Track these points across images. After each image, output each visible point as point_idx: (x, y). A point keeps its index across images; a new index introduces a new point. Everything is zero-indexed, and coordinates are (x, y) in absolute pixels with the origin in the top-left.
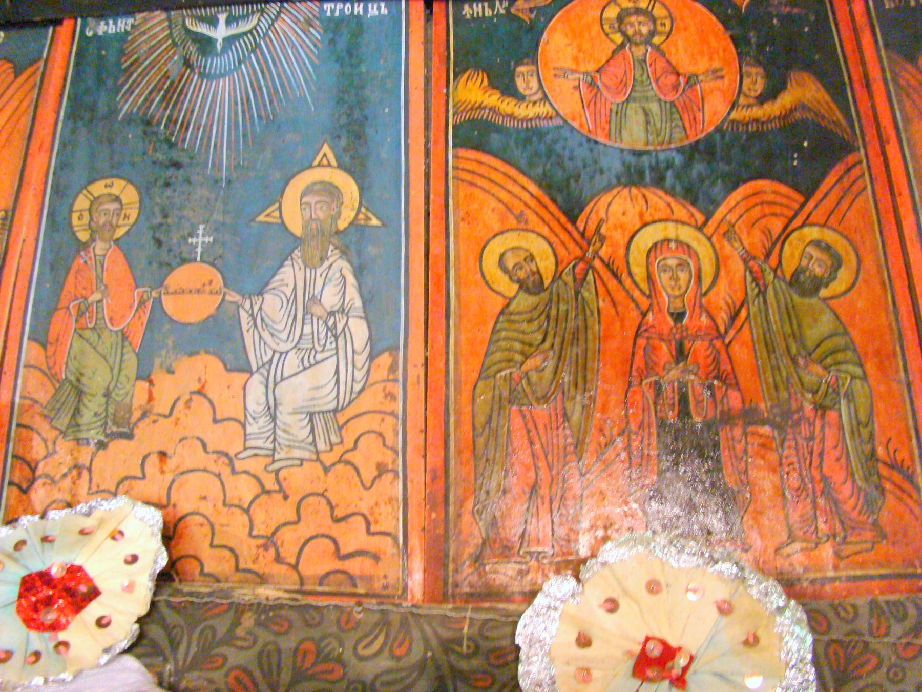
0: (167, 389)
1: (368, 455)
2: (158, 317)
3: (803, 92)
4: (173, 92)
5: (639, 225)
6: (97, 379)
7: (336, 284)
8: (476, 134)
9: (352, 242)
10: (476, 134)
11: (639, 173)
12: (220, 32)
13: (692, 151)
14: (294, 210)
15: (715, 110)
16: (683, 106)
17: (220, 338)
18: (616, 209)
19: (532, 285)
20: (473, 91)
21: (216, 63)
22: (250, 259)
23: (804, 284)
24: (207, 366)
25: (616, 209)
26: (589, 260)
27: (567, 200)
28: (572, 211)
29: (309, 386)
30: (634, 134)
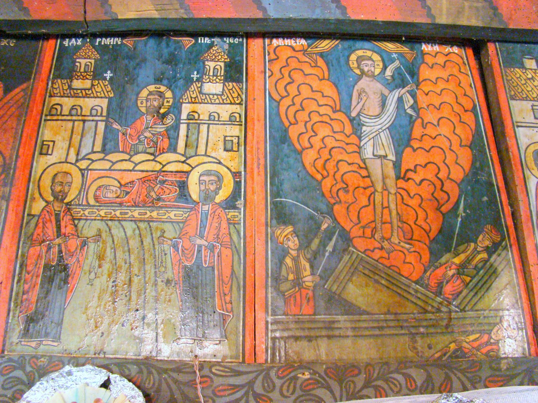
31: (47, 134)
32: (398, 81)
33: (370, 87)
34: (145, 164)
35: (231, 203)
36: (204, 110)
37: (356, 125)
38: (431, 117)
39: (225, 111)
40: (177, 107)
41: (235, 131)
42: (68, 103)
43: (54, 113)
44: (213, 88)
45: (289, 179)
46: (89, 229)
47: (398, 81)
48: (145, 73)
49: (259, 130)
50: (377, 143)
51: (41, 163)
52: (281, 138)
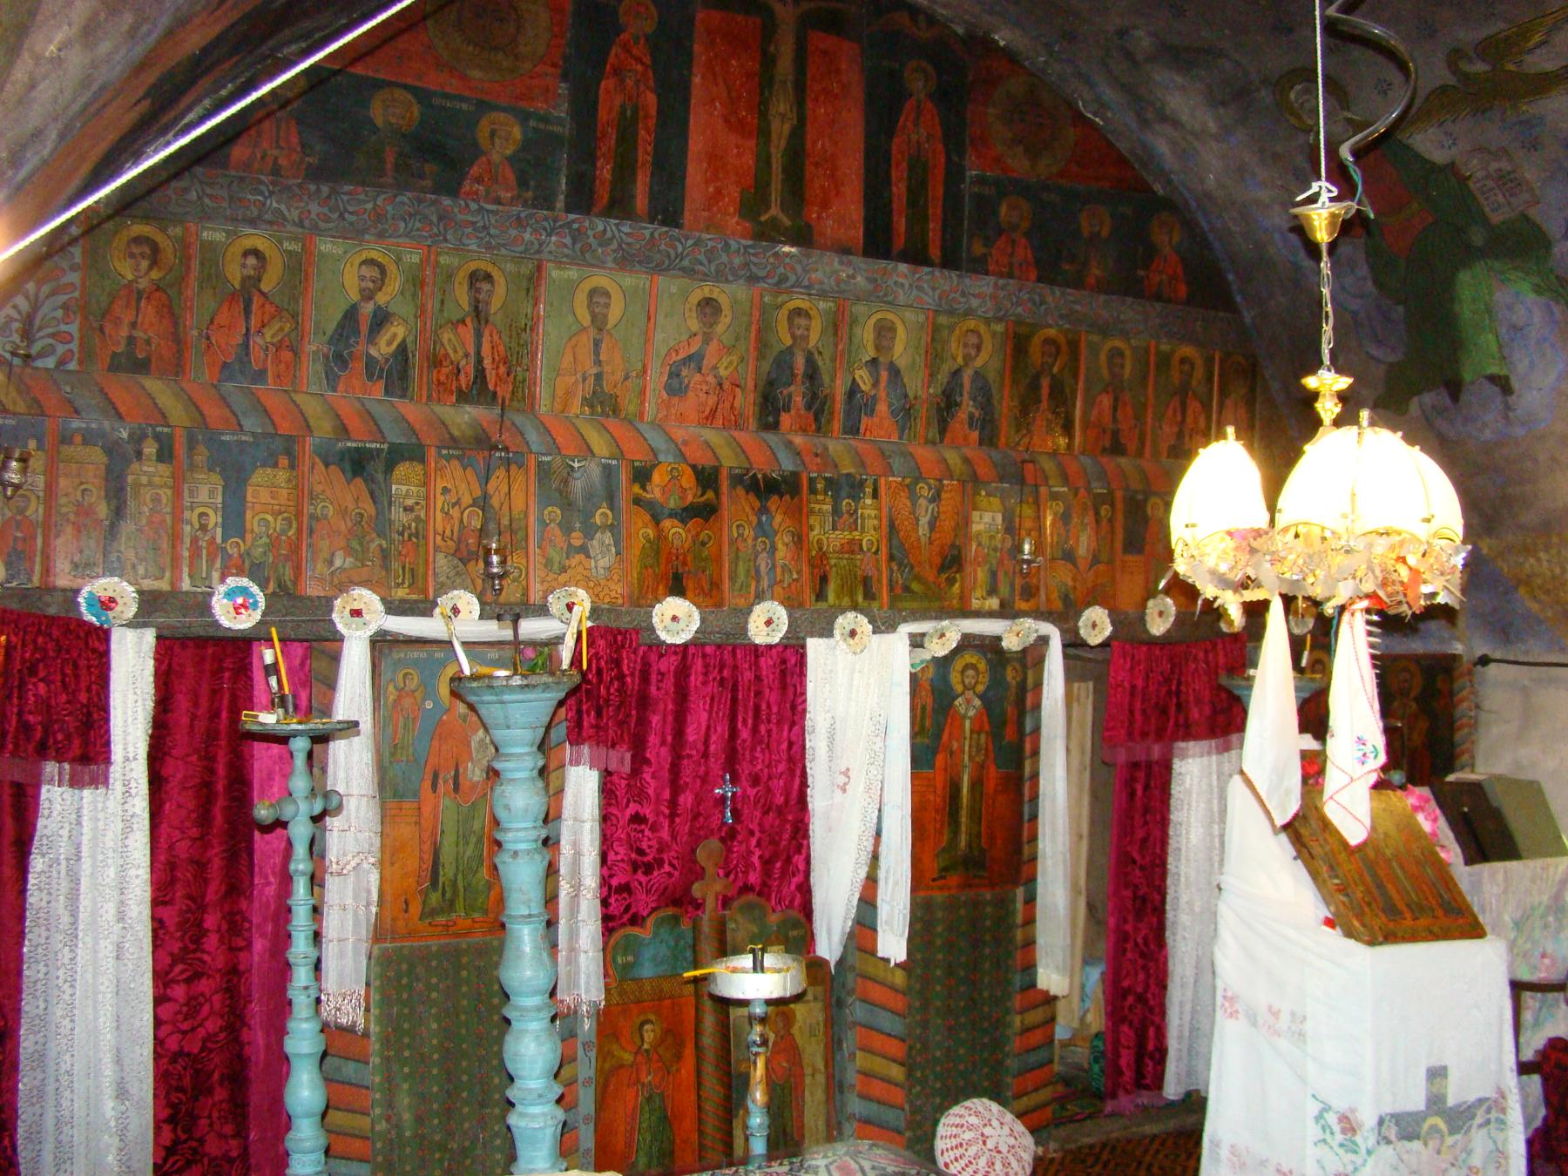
0: (574, 562)
1: (616, 577)
2: (570, 545)
3: (710, 495)
4: (566, 482)
5: (675, 530)
6: (557, 559)
7: (608, 538)
8: (637, 501)
9: (612, 528)
10: (637, 501)
11: (672, 515)
12: (576, 465)
13: (684, 509)
14: (598, 519)
15: (690, 498)
16: (683, 498)
17: (584, 550)
18: (667, 523)
19: (649, 541)
20: (637, 489)
21: (576, 475)
22: (589, 531)
23: (703, 544)
24: (580, 557)
25: (667, 523)
26: (661, 536)
27: (656, 520)
28: (658, 524)
29: (604, 562)
30: (672, 504)
31: (811, 521)
32: (932, 500)
33: (923, 502)
34: (847, 535)
35: (876, 553)
36: (867, 512)
37: (917, 520)
38: (943, 517)
39: (873, 513)
40: (856, 511)
41: (876, 522)
42: (817, 507)
43: (812, 512)
44: (869, 501)
45: (895, 542)
46: (833, 562)
47: (932, 500)
48: (844, 493)
49: (885, 522)
50: (923, 530)
51: (812, 534)
52: (892, 526)
